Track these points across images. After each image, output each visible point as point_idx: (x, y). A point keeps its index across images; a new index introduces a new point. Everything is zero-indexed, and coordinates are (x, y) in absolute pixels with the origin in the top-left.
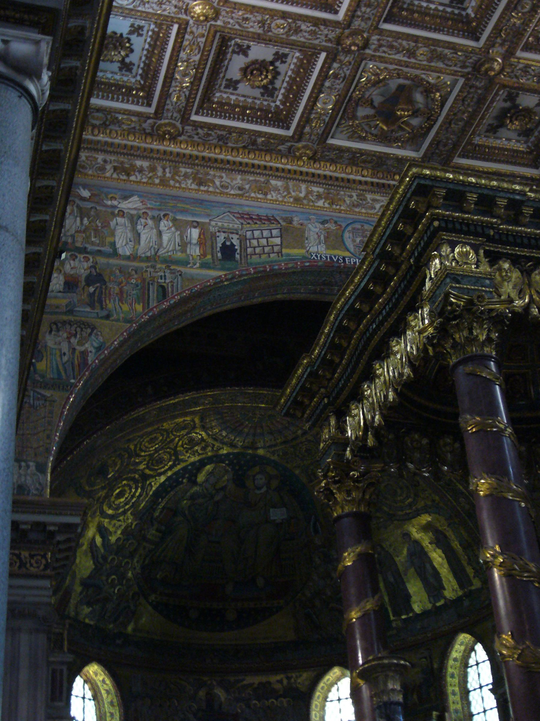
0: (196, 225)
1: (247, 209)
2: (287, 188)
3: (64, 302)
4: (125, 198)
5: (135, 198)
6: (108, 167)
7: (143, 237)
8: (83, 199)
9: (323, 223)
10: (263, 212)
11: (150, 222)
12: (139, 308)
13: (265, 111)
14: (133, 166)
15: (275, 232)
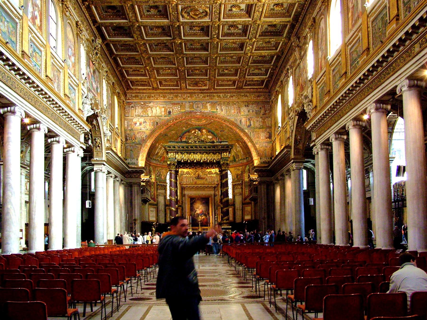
0: (163, 107)
1: (174, 102)
2: (182, 96)
3: (140, 128)
4: (150, 103)
5: (152, 103)
6: (146, 97)
7: (153, 112)
8: (142, 105)
9: (189, 103)
10: (177, 102)
11: (155, 108)
12: (153, 127)
13: (174, 85)
14: (151, 96)
15: (179, 107)
